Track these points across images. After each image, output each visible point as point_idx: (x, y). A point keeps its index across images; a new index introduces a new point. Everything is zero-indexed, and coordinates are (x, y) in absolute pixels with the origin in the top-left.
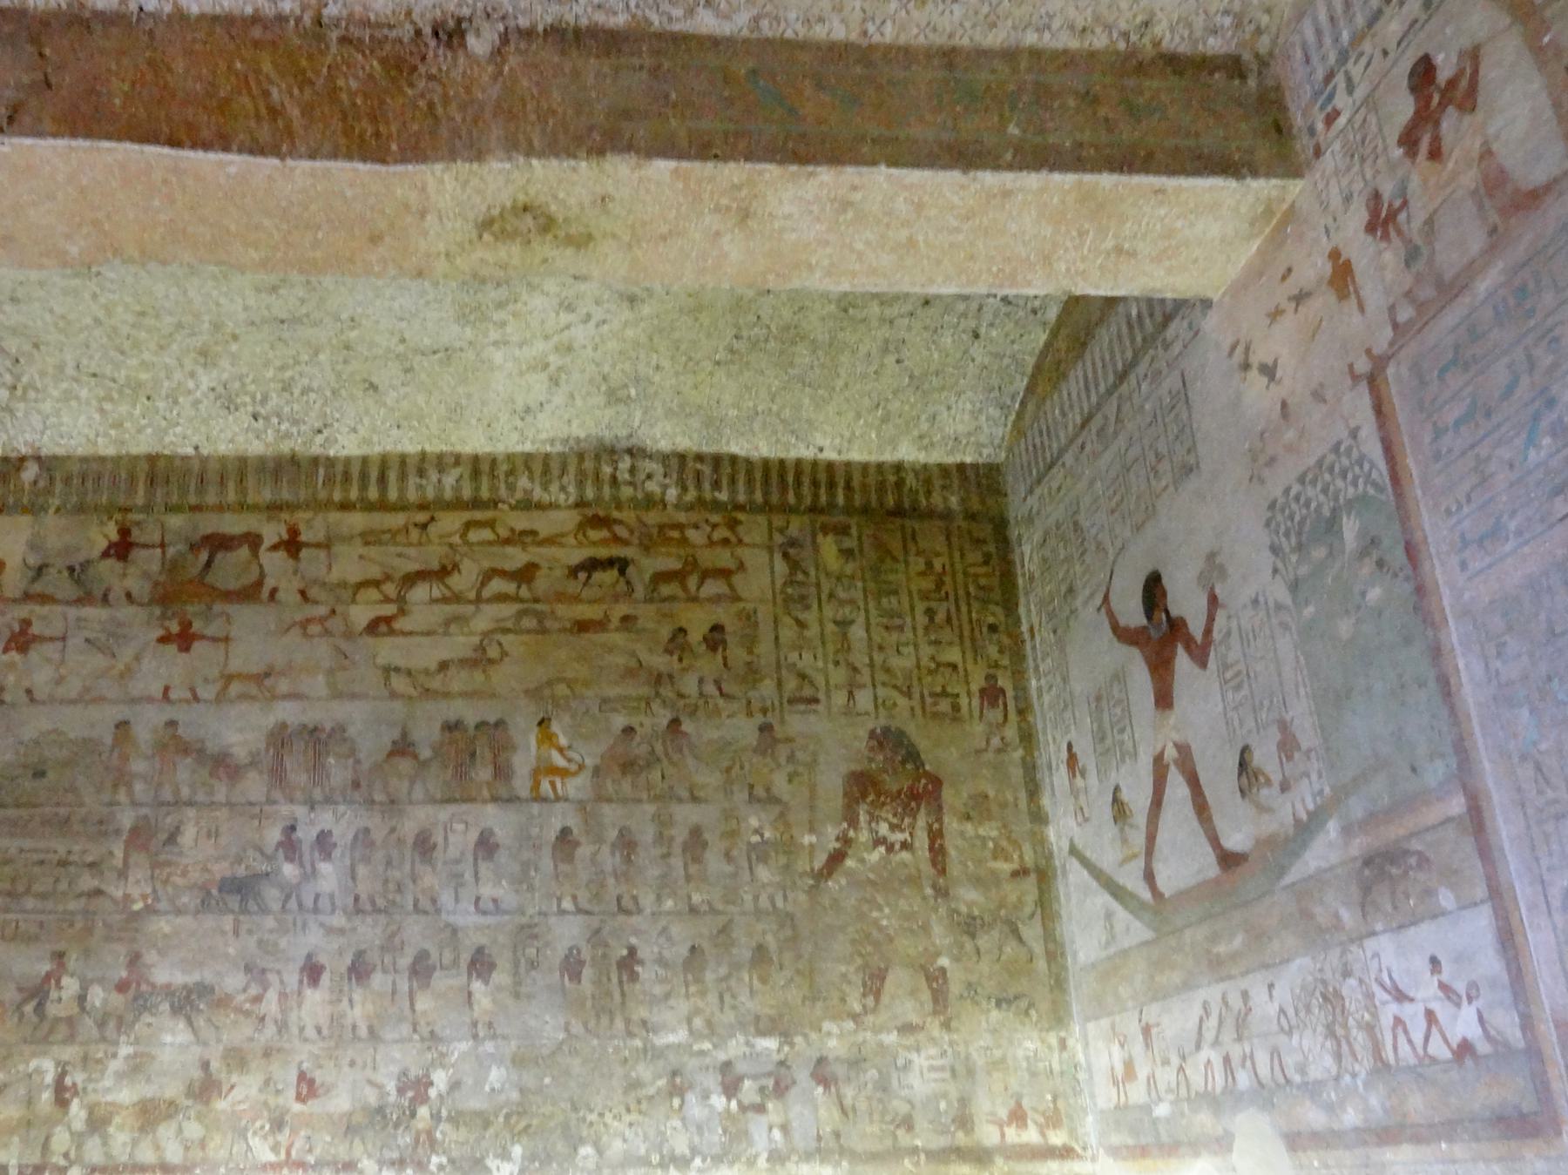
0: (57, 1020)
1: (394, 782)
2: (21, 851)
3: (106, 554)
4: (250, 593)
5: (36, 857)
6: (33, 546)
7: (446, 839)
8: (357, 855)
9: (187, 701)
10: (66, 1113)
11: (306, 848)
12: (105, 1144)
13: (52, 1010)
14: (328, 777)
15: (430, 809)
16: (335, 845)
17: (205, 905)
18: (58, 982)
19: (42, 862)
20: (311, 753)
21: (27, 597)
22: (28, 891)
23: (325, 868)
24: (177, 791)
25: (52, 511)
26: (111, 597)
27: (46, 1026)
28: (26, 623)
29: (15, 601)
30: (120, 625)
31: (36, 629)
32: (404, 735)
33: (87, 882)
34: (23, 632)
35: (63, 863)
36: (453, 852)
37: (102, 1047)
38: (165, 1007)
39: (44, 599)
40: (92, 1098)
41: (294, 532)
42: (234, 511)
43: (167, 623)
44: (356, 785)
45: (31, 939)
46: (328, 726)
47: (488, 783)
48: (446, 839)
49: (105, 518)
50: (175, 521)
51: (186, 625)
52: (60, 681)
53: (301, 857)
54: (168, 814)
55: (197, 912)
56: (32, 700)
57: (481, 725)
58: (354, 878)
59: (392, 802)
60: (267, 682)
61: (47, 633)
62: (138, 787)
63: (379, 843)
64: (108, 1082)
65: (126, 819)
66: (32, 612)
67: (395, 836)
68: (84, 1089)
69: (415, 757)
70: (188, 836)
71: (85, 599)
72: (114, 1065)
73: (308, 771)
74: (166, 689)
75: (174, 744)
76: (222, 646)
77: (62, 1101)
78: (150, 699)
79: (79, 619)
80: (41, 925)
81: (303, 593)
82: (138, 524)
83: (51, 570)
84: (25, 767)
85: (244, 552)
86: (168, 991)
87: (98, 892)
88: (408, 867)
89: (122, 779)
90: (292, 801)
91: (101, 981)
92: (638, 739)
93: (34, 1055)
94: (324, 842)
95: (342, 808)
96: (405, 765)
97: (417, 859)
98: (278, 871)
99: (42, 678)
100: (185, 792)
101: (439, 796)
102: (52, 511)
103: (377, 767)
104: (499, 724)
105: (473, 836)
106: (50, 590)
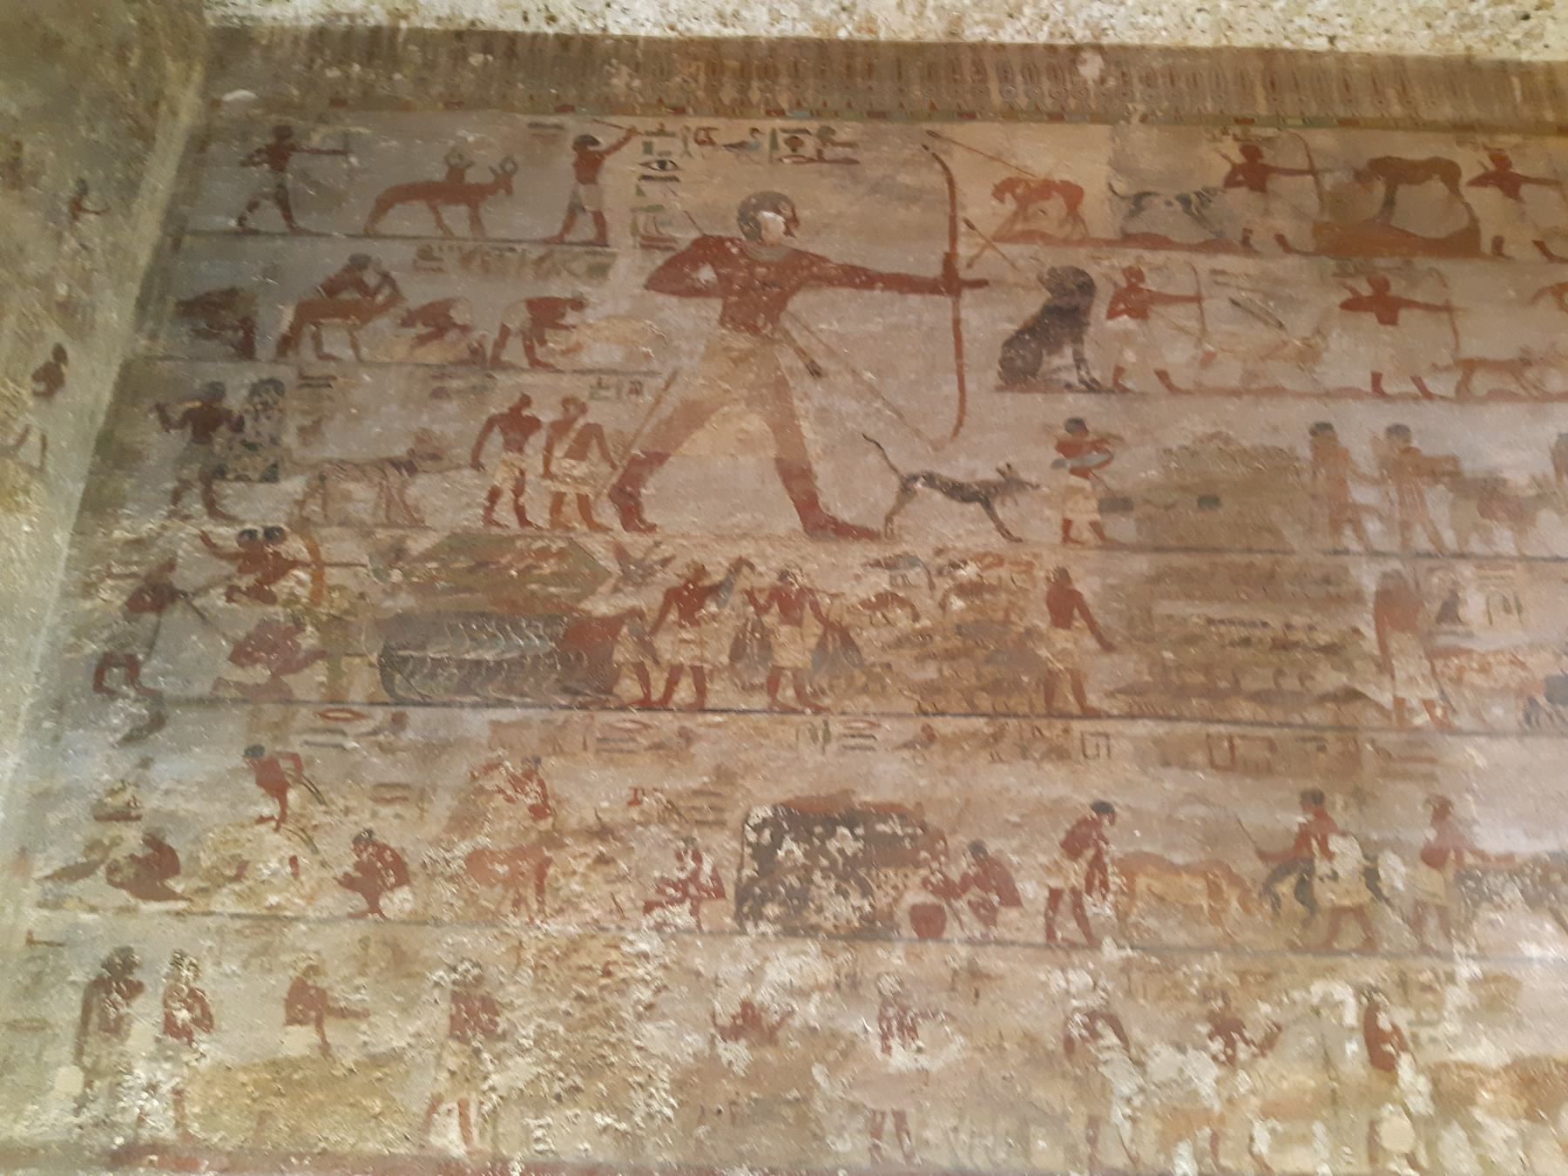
0: (1338, 912)
2: (1210, 621)
3: (1230, 182)
4: (1464, 244)
5: (1238, 632)
6: (1119, 166)
9: (1415, 398)
10: (1394, 1081)
12: (1474, 1141)
13: (1326, 895)
17: (1531, 723)
18: (1323, 845)
19: (1246, 642)
21: (1127, 239)
22: (1236, 690)
24: (1435, 537)
25: (1135, 120)
26: (1253, 240)
27: (1322, 921)
28: (1134, 275)
29: (1110, 243)
30: (1278, 281)
31: (1151, 283)
33: (1329, 679)
34: (1132, 288)
35: (1282, 645)
37: (1426, 961)
38: (1513, 893)
39: (1155, 242)
40: (1433, 1055)
41: (1500, 159)
42: (1405, 129)
43: (1350, 282)
45: (1261, 770)
49: (1217, 132)
50: (1323, 140)
51: (1381, 287)
52: (1208, 360)
54: (1431, 570)
55: (1524, 734)
56: (1172, 389)
60: (1530, 374)
61: (1171, 290)
62: (1373, 526)
64: (1451, 1027)
65: (1368, 579)
66: (1139, 258)
68: (1415, 1037)
70: (1474, 606)
71: (1215, 245)
72: (1457, 996)
74: (1376, 379)
75: (1408, 465)
76: (1444, 316)
77: (1382, 1063)
78: (1357, 394)
79: (1215, 272)
80: (1271, 746)
81: (1540, 245)
82: (1268, 140)
83: (1156, 200)
84: (1183, 488)
85: (1437, 187)
86: (1509, 866)
87: (1352, 695)
89: (1344, 515)
91: (1398, 847)
93: (1315, 974)
99: (1178, 356)
100: (1449, 538)
102: (1135, 120)
106: (1161, 230)
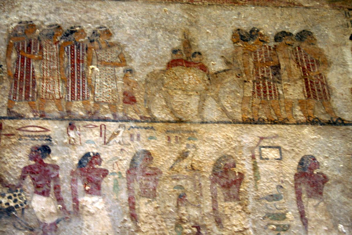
1: (179, 97)
7: (255, 168)
8: (136, 186)
11: (63, 175)
14: (92, 88)
15: (230, 131)
16: (105, 173)
20: (67, 60)
23: (92, 203)
32: (187, 43)
36: (267, 186)
44: (130, 99)
46: (89, 28)
47: (301, 103)
48: (255, 168)
53: (57, 188)
57: (280, 36)
58: (134, 217)
59: (180, 121)
63: (165, 171)
67: (185, 163)
69: (203, 68)
73: (64, 81)
88: (208, 204)
90: (43, 117)
94: (90, 169)
95: (112, 127)
96: (191, 77)
97: (220, 193)
98: (26, 206)
101: (239, 117)
103: (154, 79)
104: (304, 35)
105: (291, 166)
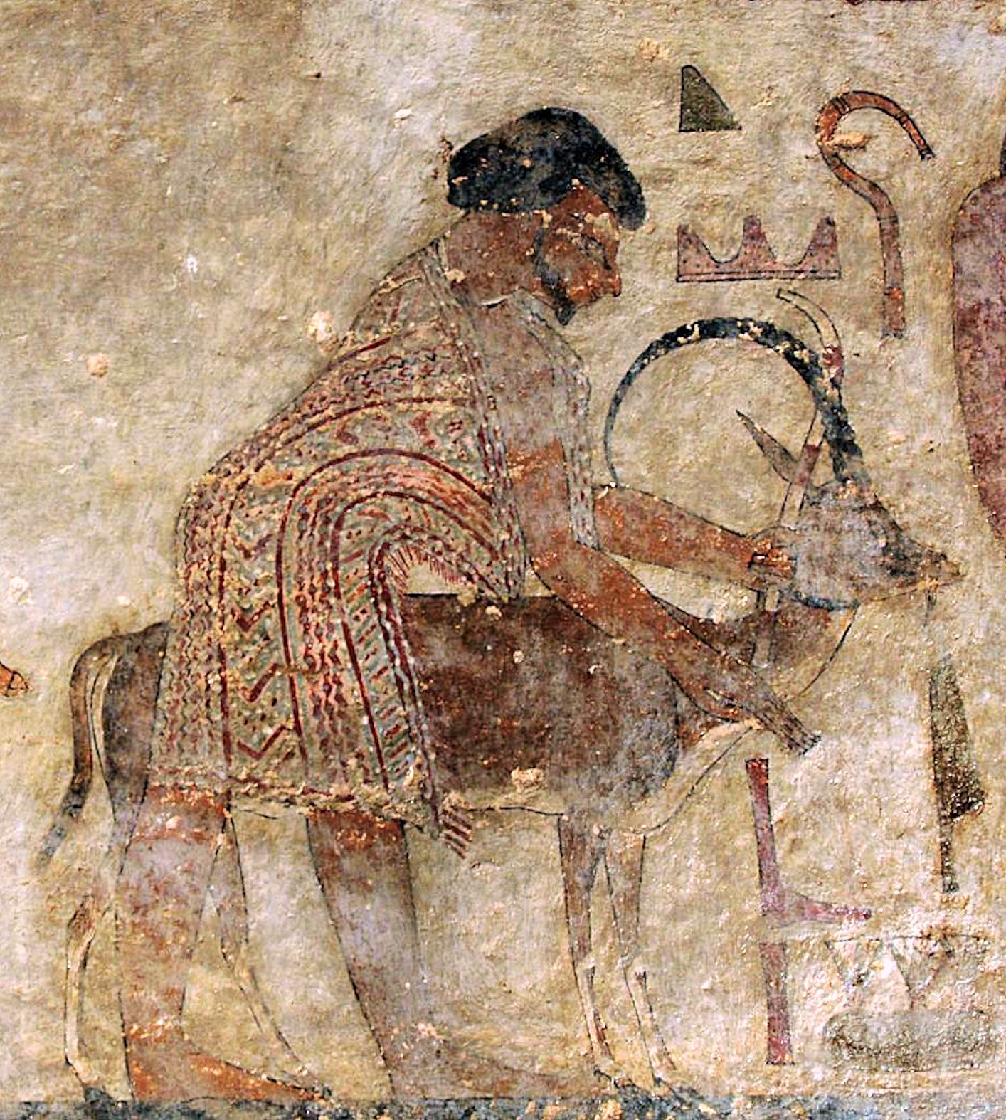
92: (650, 291)
